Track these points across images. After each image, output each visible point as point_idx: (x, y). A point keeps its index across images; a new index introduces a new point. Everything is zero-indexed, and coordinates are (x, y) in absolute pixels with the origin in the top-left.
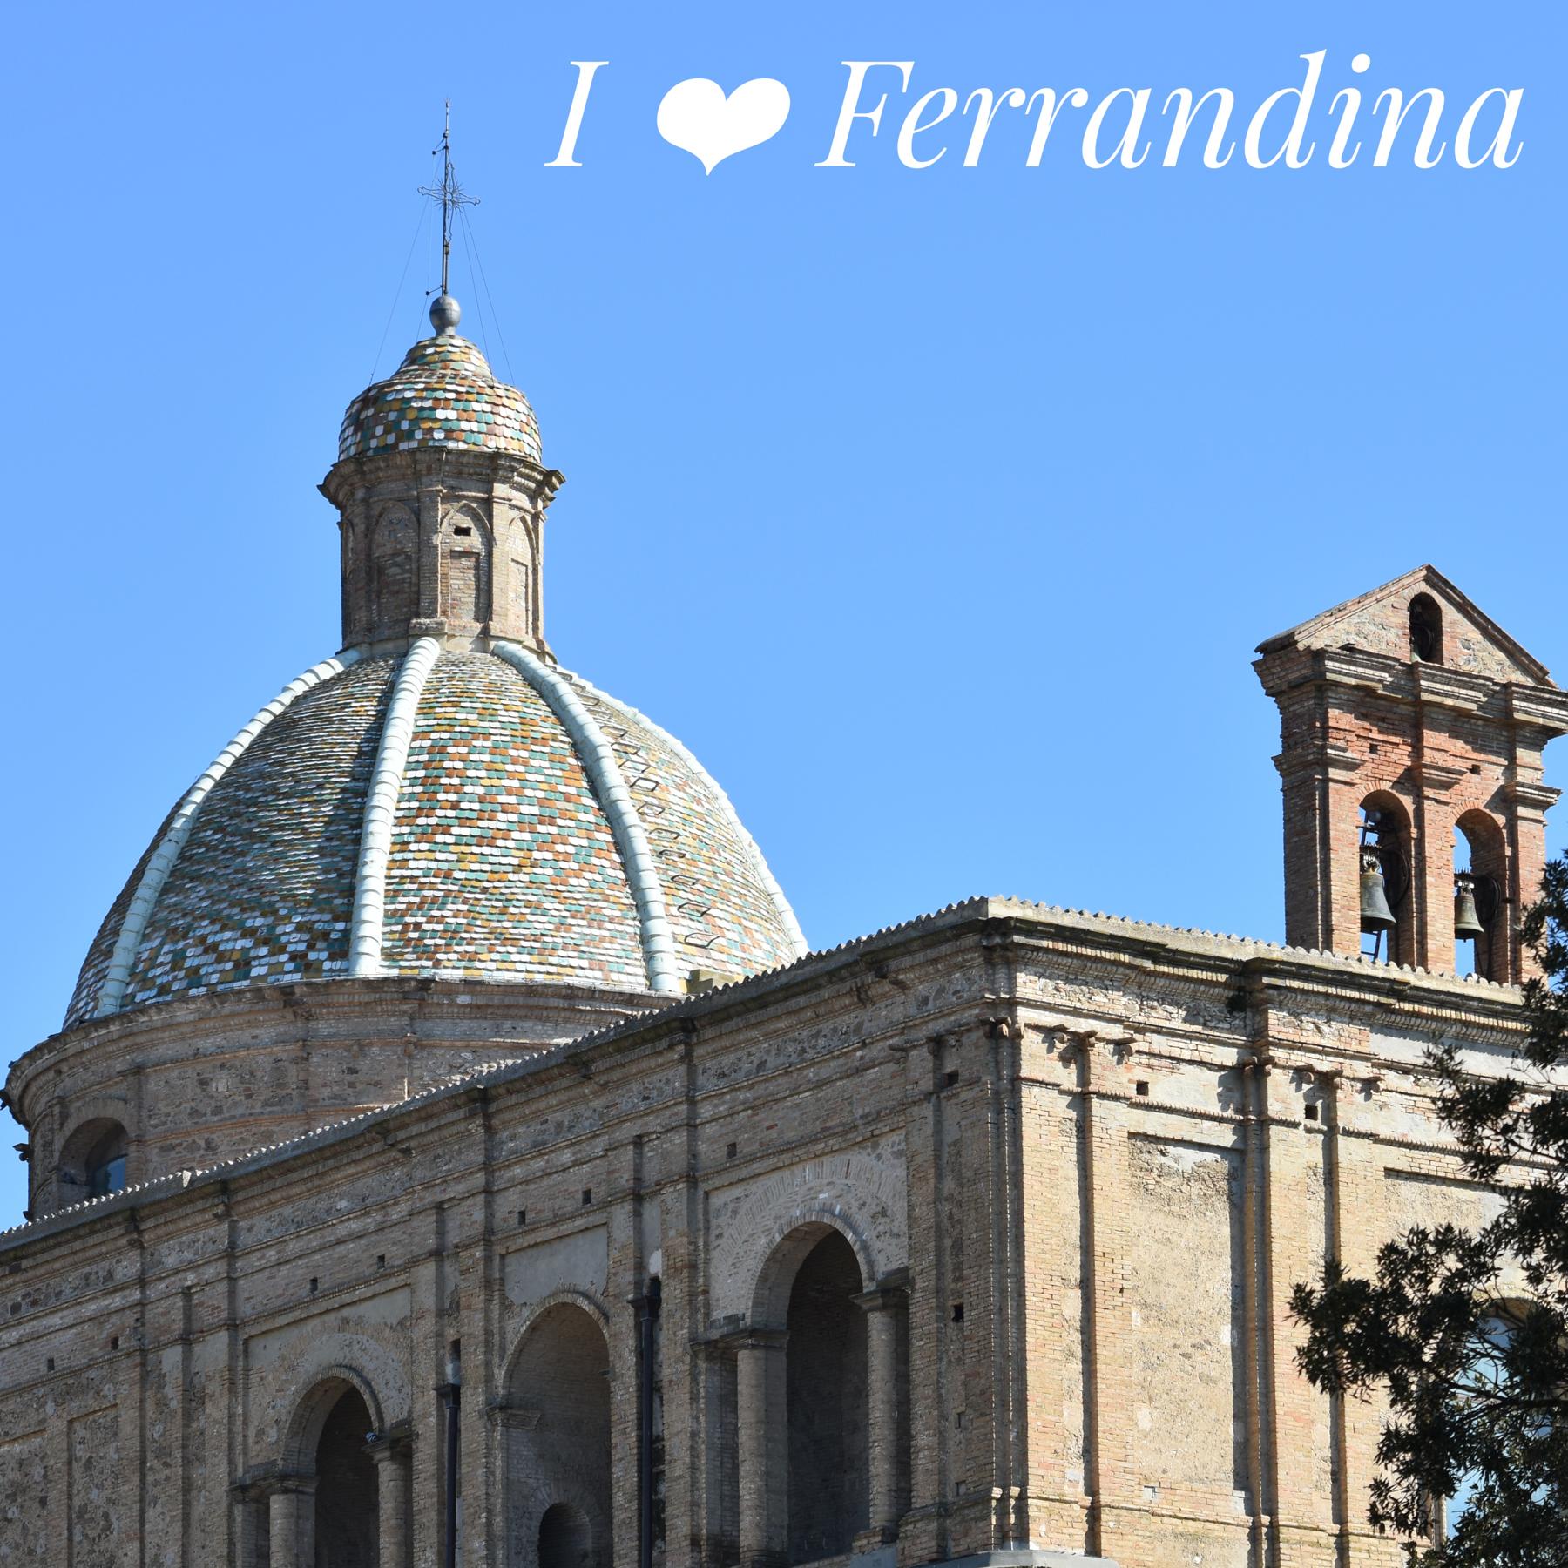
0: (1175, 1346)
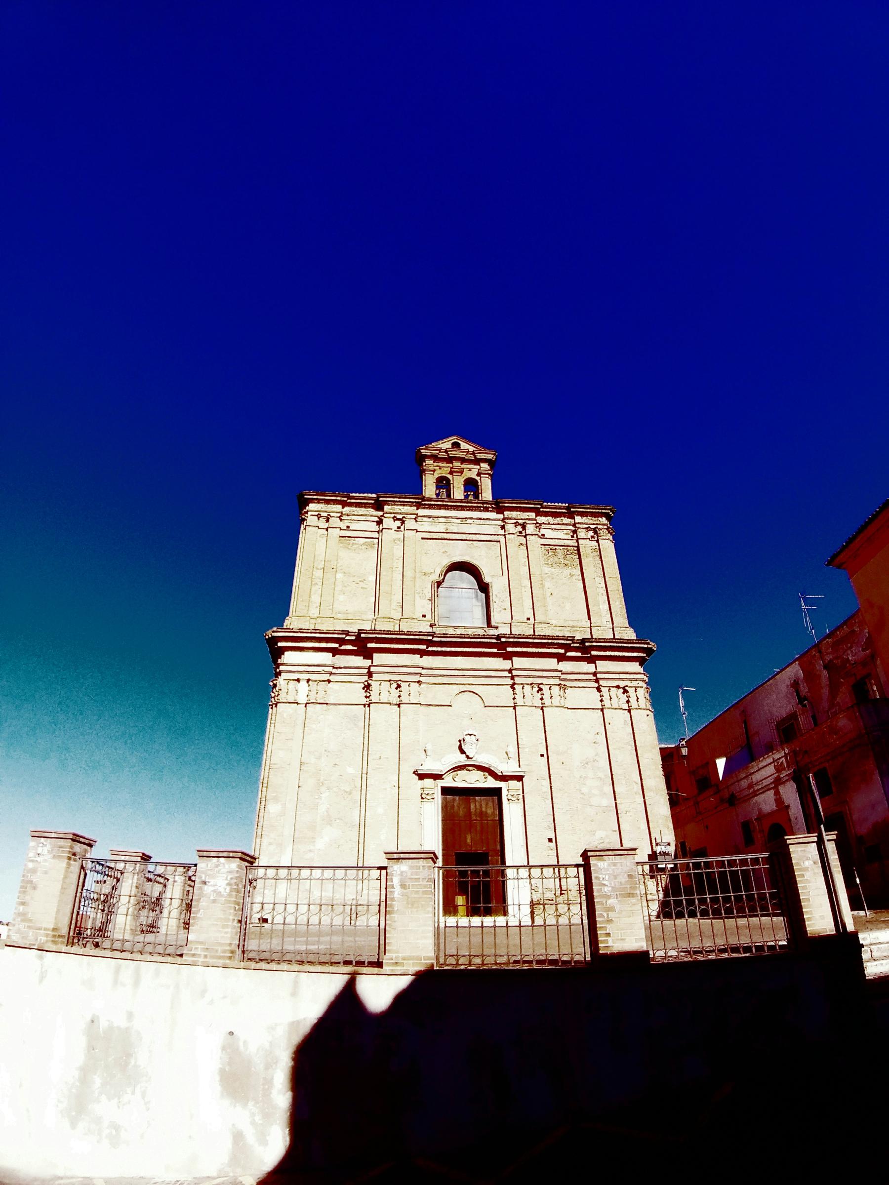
0: (354, 581)
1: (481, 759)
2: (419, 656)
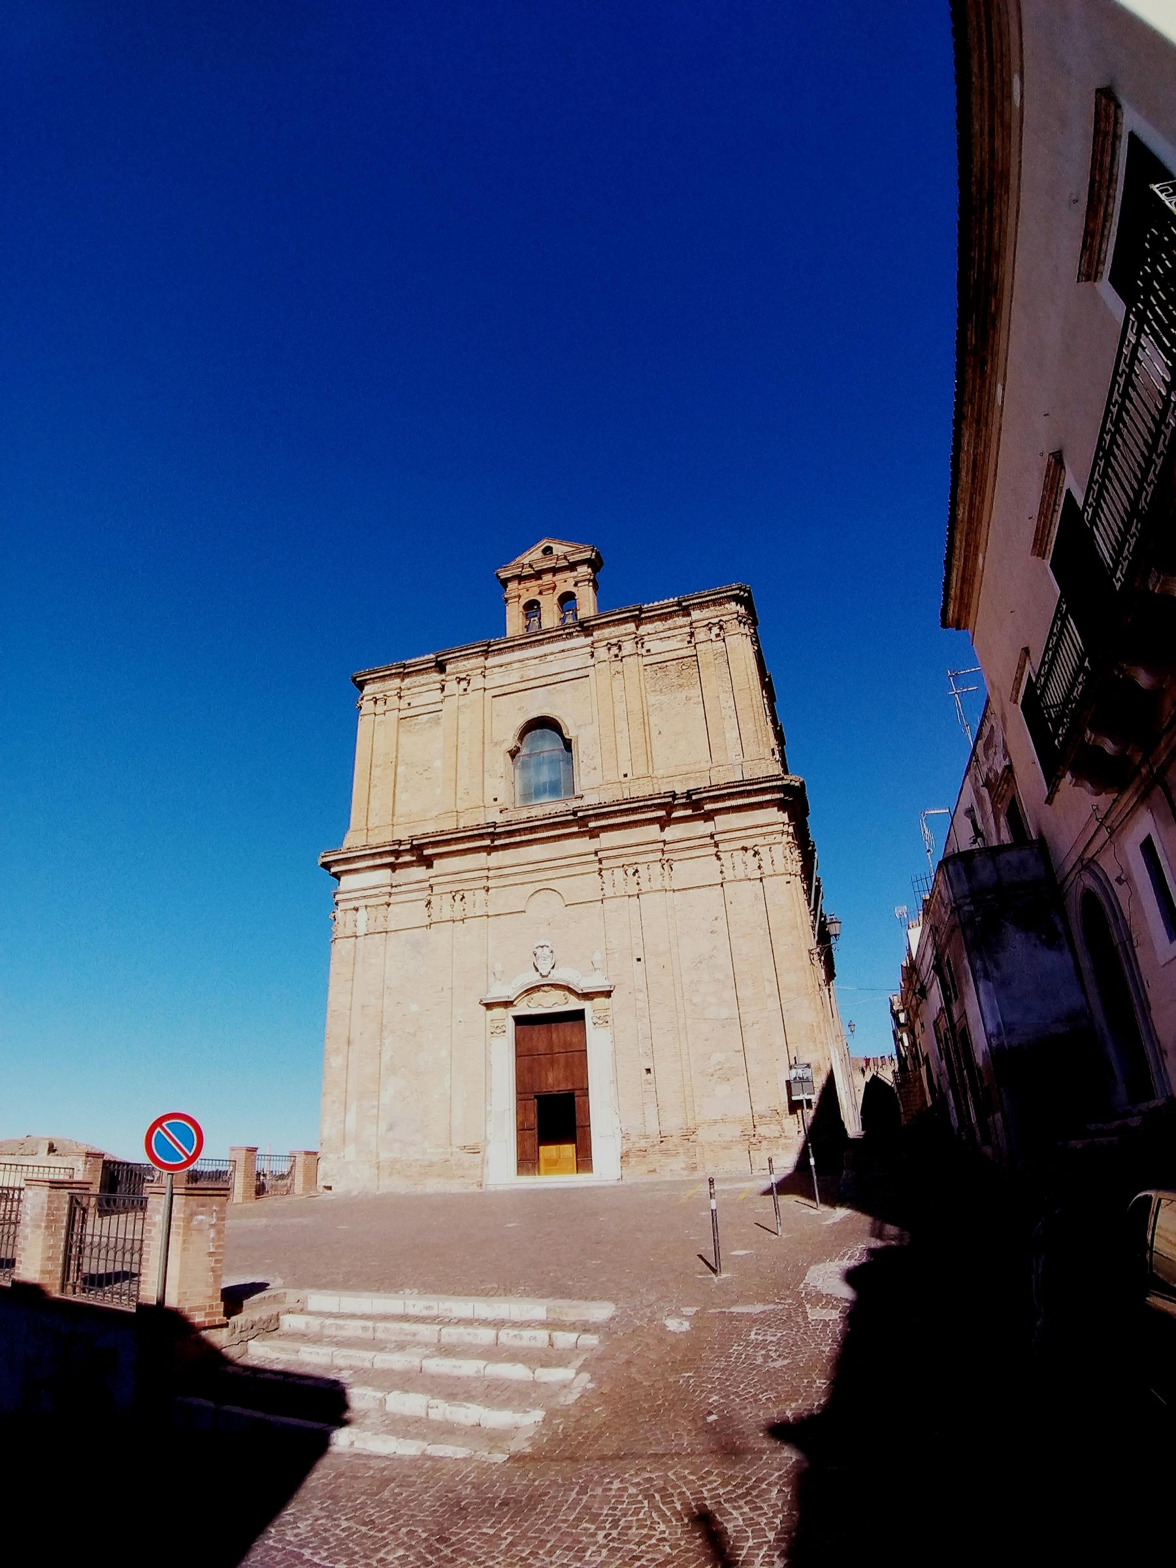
2: (485, 854)
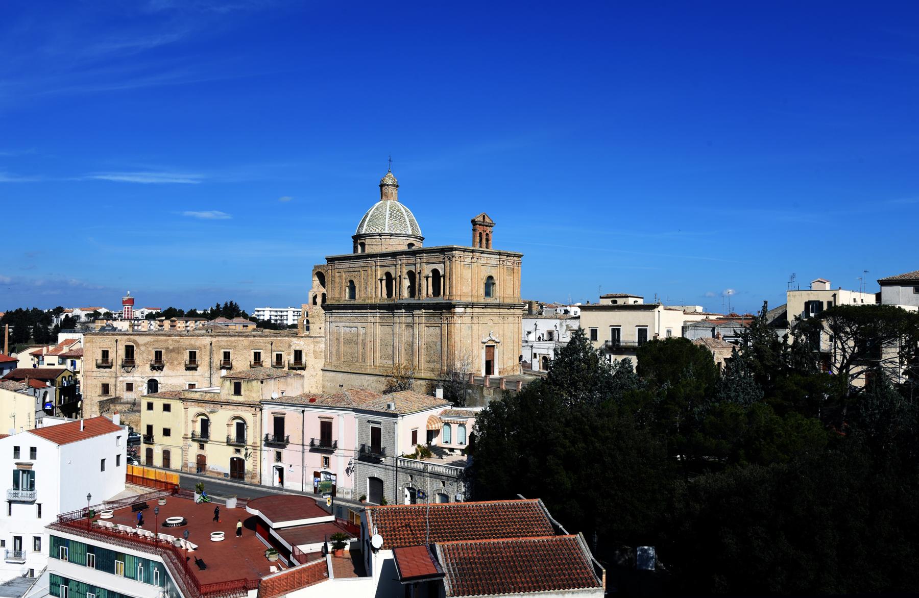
1: (493, 338)
